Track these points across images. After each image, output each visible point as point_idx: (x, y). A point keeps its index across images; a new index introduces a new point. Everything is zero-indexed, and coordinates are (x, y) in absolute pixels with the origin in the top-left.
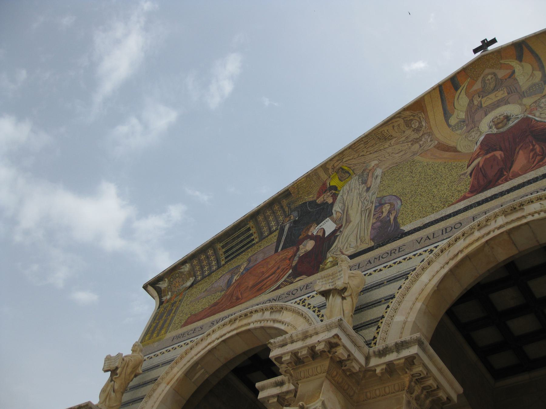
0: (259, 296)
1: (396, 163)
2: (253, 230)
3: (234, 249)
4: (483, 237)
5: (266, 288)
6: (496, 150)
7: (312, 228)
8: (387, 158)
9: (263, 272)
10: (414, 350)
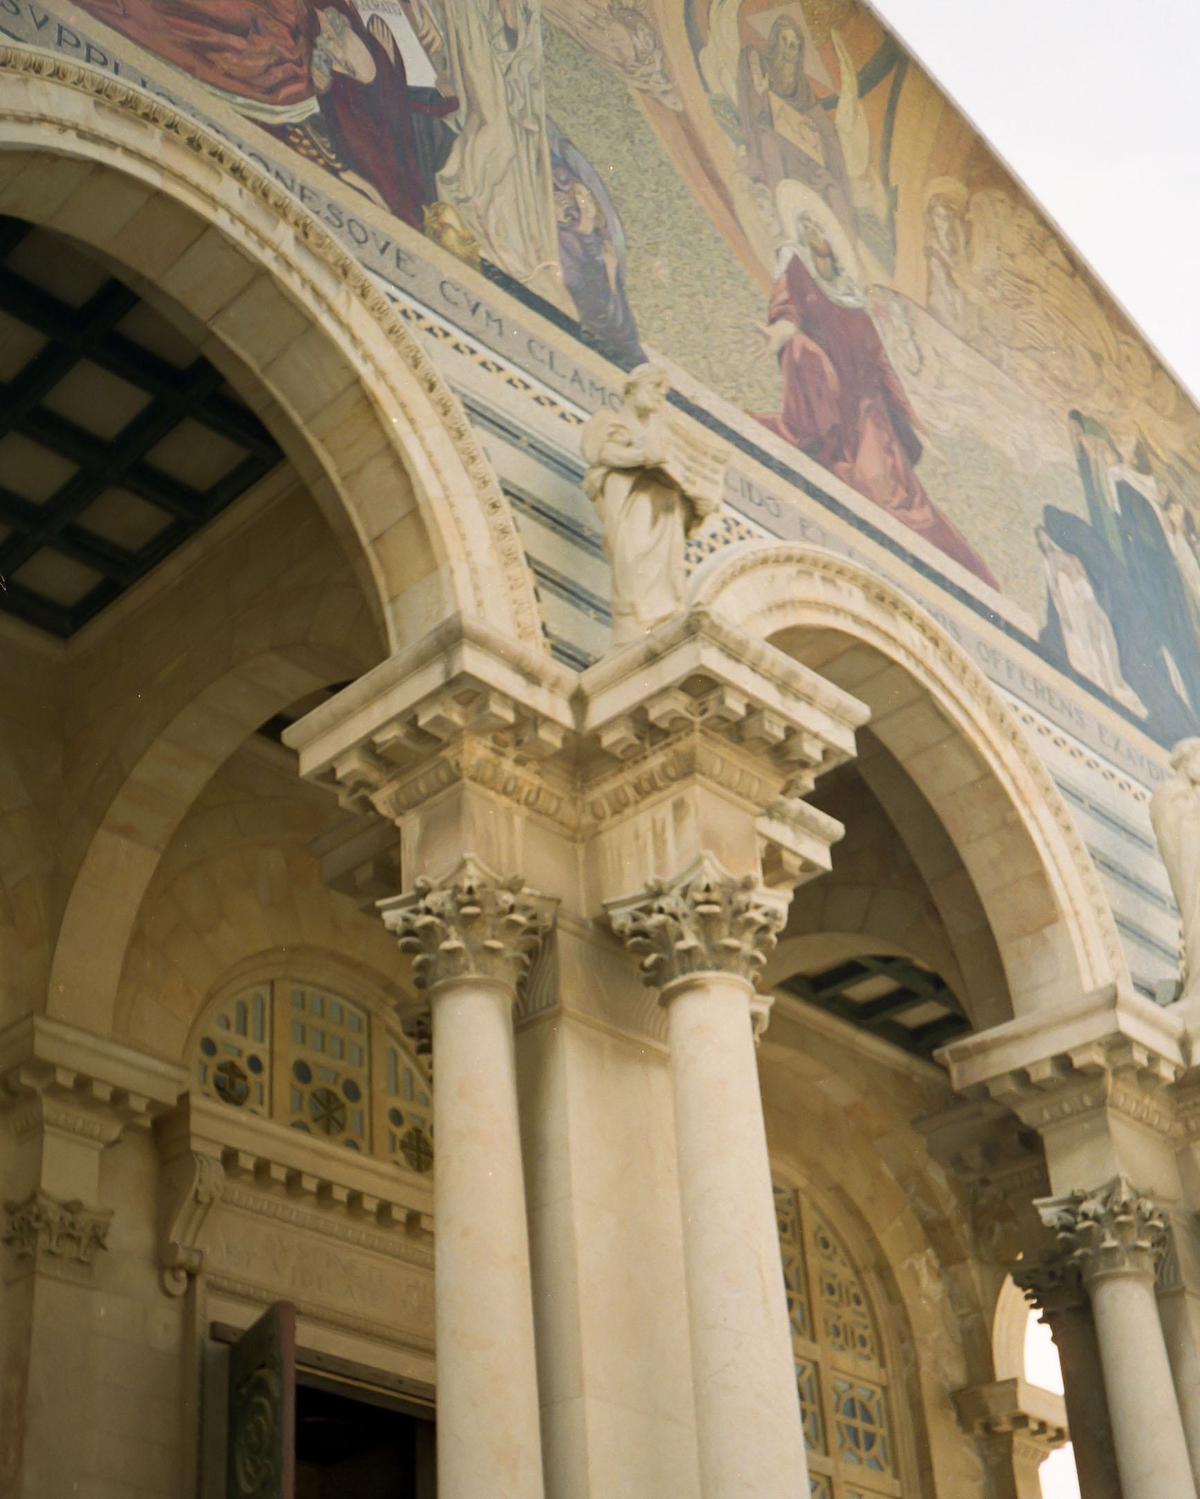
0: (208, 88)
5: (229, 75)
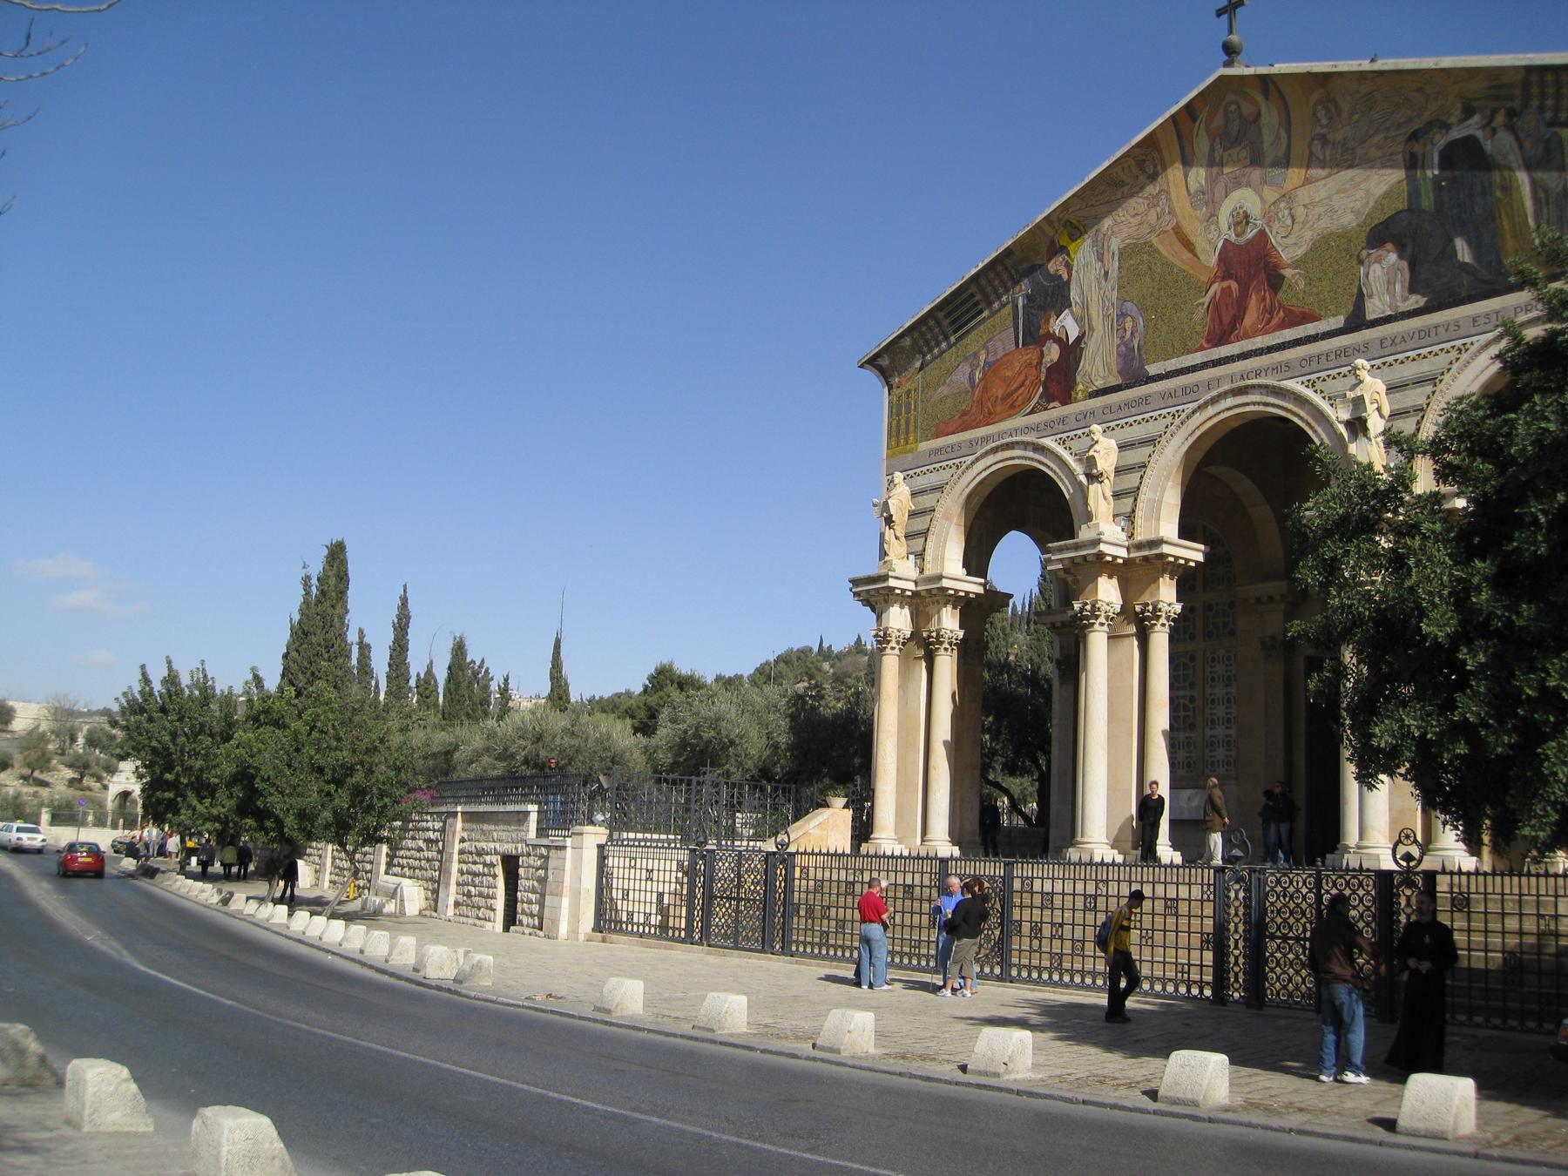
2: (978, 297)
4: (1215, 415)
6: (1230, 277)
7: (1052, 320)
8: (1123, 219)
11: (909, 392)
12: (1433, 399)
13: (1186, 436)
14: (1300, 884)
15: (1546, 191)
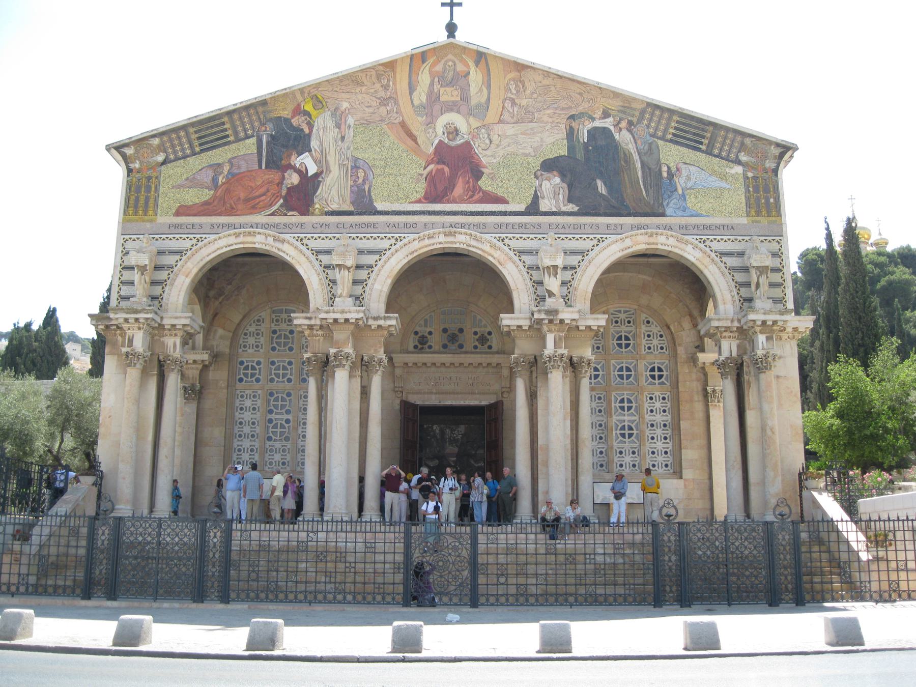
1: (366, 121)
2: (227, 126)
3: (208, 139)
6: (444, 163)
7: (293, 157)
9: (251, 187)
10: (393, 322)
11: (149, 178)
12: (582, 264)
13: (406, 253)
14: (714, 531)
15: (650, 169)
